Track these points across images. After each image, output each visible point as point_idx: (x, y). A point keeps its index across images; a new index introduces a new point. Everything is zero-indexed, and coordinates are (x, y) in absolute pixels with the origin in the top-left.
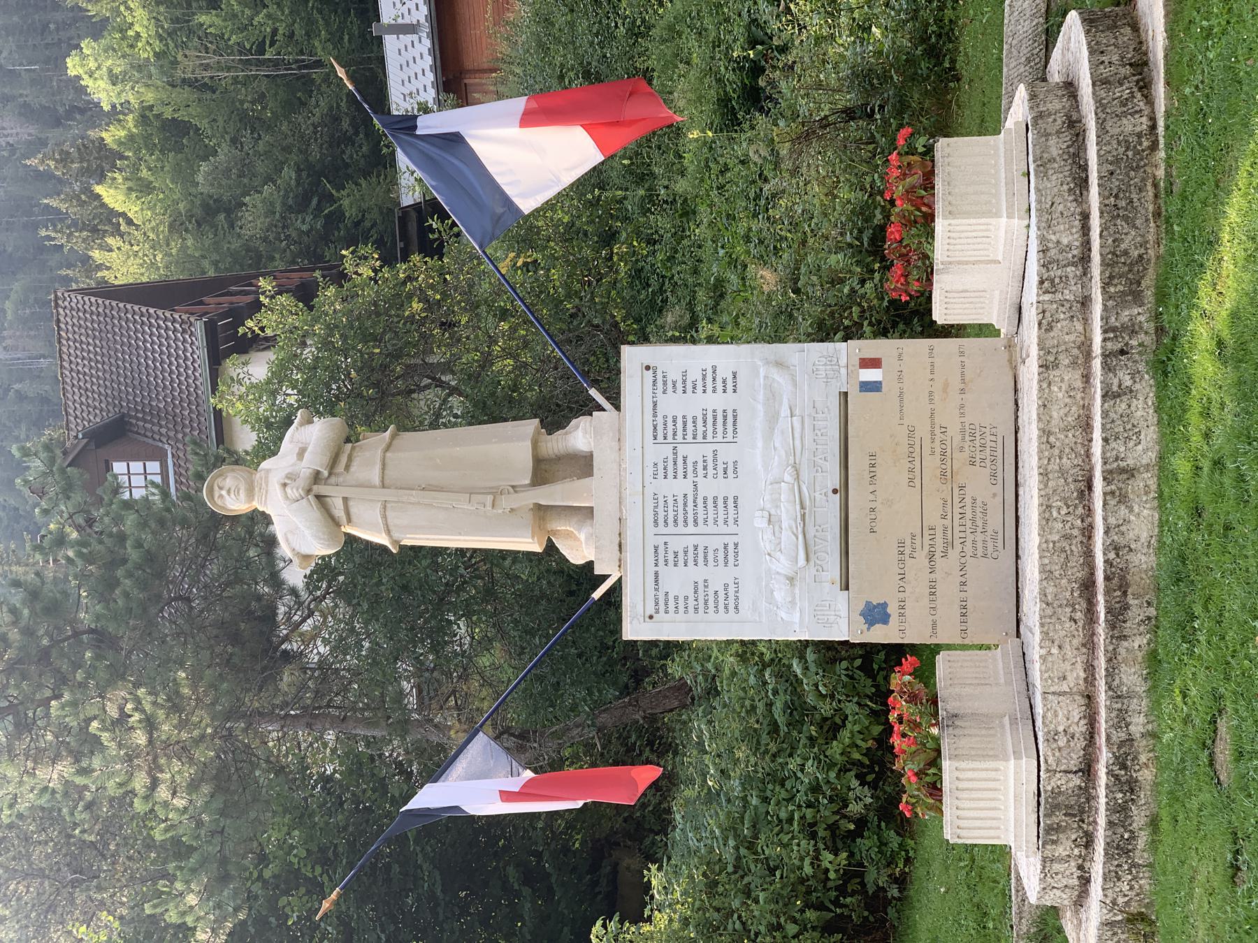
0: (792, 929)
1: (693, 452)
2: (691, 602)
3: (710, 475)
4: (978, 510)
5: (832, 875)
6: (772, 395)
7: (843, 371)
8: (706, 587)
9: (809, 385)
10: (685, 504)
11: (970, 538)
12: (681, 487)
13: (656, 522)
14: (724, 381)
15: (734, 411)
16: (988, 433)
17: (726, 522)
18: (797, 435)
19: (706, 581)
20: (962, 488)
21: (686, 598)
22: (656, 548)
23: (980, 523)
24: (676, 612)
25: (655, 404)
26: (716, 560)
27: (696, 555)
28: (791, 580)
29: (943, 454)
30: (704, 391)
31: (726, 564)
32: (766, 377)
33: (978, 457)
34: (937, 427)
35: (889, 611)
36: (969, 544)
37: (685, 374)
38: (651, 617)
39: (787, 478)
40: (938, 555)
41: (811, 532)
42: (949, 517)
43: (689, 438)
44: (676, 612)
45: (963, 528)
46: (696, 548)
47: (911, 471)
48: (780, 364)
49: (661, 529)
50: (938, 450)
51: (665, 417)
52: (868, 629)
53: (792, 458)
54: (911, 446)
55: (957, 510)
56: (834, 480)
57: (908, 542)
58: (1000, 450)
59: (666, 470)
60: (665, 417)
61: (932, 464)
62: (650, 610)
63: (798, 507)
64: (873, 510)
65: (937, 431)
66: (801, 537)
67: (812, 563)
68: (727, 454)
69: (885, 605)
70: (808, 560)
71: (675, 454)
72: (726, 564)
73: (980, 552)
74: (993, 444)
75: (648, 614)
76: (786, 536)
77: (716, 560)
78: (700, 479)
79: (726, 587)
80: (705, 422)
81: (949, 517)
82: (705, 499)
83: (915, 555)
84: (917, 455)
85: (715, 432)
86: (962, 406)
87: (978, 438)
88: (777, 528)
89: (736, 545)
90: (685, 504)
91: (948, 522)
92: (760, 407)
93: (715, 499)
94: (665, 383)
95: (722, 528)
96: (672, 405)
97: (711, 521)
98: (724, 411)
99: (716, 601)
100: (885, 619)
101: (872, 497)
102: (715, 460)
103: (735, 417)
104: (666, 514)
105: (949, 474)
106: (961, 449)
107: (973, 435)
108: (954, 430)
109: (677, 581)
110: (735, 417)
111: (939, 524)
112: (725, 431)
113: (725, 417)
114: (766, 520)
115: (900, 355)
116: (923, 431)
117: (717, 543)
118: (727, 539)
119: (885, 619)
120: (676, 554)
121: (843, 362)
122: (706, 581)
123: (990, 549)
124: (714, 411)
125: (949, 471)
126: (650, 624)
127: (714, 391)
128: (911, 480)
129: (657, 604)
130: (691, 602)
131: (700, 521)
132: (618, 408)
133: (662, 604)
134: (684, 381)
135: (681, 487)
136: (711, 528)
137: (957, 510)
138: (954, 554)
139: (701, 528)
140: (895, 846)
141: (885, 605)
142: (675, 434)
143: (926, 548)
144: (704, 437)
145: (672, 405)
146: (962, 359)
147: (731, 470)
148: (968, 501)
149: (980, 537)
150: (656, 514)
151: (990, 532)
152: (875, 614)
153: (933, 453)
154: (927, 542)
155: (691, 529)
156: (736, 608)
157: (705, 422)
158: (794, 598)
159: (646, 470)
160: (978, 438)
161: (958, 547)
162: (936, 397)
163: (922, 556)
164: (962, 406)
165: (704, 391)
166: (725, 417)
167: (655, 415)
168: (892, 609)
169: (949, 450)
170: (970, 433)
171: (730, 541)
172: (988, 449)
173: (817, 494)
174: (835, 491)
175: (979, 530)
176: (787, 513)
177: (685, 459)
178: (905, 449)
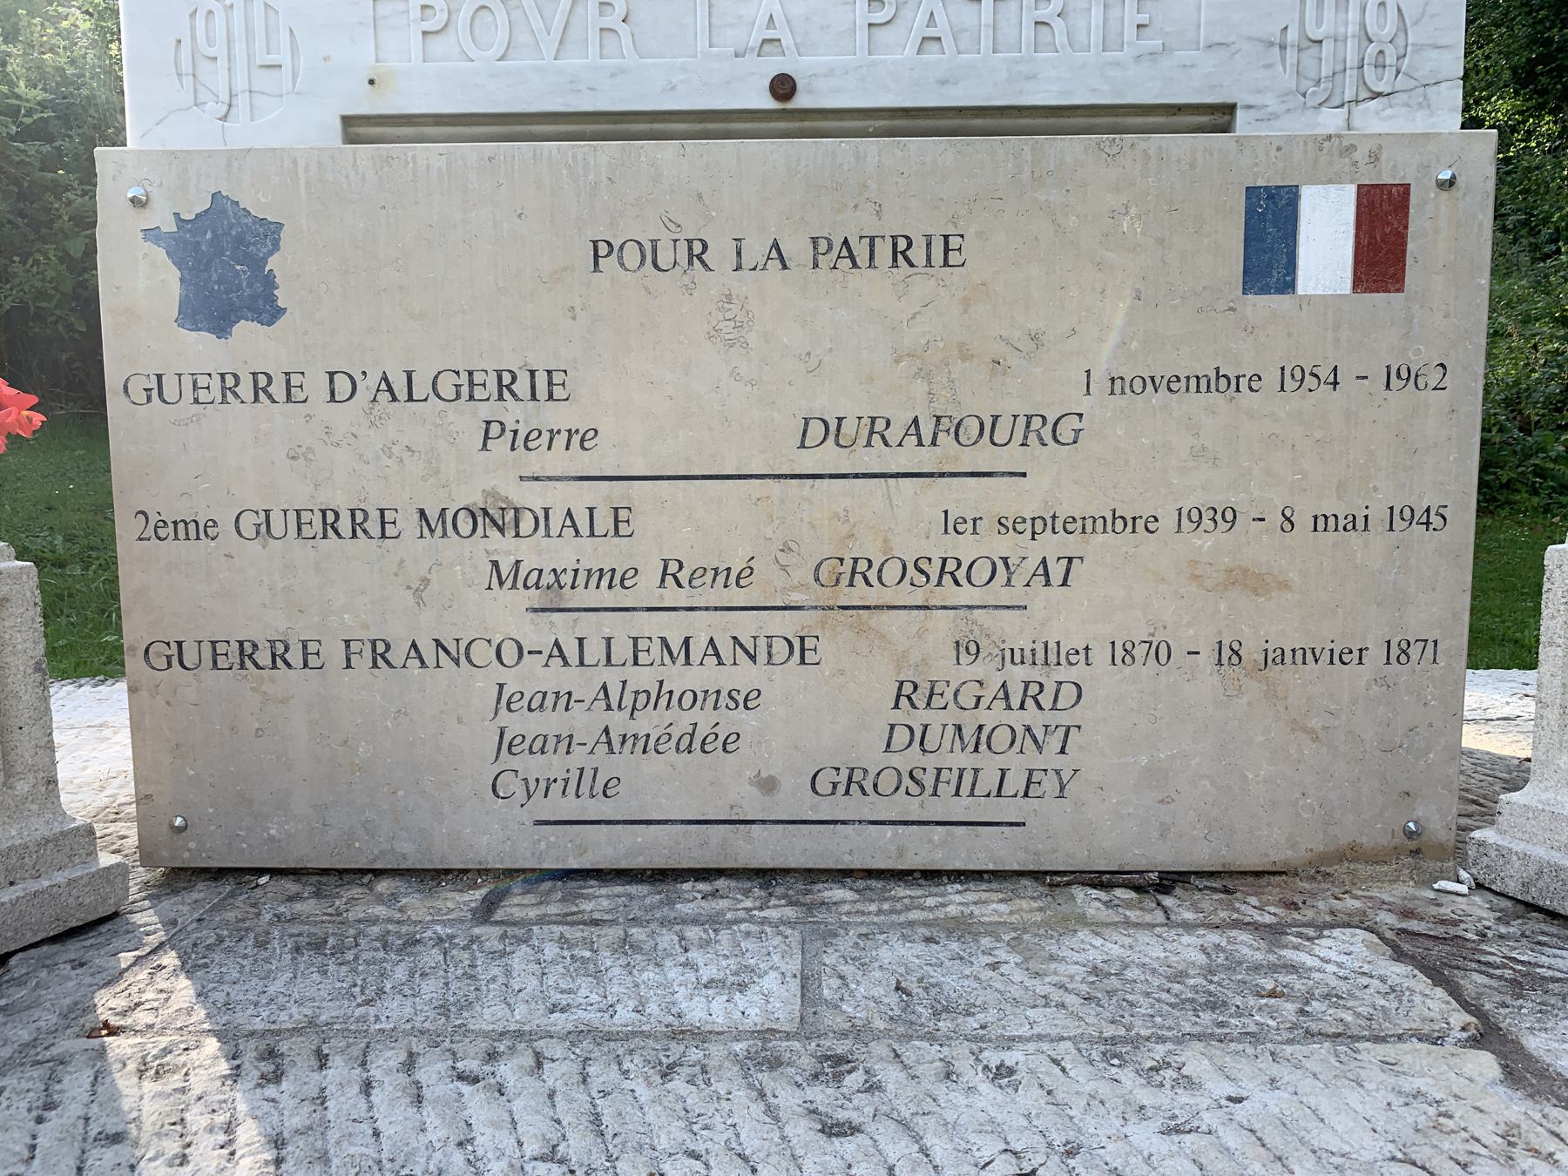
4: (704, 719)
11: (583, 683)
16: (1038, 762)
20: (800, 649)
23: (648, 722)
29: (950, 571)
33: (935, 718)
34: (1072, 544)
35: (244, 329)
36: (555, 678)
40: (504, 548)
42: (672, 596)
45: (622, 651)
47: (876, 429)
50: (966, 548)
52: (152, 234)
54: (988, 429)
55: (701, 628)
57: (557, 416)
58: (961, 808)
61: (904, 520)
64: (697, 254)
65: (1052, 545)
69: (269, 312)
73: (519, 723)
74: (989, 781)
81: (672, 596)
83: (500, 447)
84: (948, 453)
86: (1159, 652)
87: (1017, 719)
91: (647, 588)
101: (756, 250)
105: (860, 594)
106: (968, 648)
107: (1032, 695)
108: (1063, 617)
111: (643, 551)
115: (1411, 377)
116: (1052, 482)
121: (1374, 120)
123: (534, 766)
125: (873, 595)
128: (833, 430)
137: (701, 628)
138: (508, 615)
141: (269, 312)
143: (533, 497)
146: (1376, 654)
148: (743, 676)
149: (585, 722)
151: (611, 766)
152: (229, 269)
153: (952, 525)
154: (559, 497)
160: (1017, 719)
161: (537, 633)
162: (1205, 542)
163: (494, 476)
164: (1159, 652)
168: (251, 345)
169: (966, 595)
170: (1043, 686)
172: (965, 760)
174: (783, 87)
175: (619, 722)
178: (976, 398)
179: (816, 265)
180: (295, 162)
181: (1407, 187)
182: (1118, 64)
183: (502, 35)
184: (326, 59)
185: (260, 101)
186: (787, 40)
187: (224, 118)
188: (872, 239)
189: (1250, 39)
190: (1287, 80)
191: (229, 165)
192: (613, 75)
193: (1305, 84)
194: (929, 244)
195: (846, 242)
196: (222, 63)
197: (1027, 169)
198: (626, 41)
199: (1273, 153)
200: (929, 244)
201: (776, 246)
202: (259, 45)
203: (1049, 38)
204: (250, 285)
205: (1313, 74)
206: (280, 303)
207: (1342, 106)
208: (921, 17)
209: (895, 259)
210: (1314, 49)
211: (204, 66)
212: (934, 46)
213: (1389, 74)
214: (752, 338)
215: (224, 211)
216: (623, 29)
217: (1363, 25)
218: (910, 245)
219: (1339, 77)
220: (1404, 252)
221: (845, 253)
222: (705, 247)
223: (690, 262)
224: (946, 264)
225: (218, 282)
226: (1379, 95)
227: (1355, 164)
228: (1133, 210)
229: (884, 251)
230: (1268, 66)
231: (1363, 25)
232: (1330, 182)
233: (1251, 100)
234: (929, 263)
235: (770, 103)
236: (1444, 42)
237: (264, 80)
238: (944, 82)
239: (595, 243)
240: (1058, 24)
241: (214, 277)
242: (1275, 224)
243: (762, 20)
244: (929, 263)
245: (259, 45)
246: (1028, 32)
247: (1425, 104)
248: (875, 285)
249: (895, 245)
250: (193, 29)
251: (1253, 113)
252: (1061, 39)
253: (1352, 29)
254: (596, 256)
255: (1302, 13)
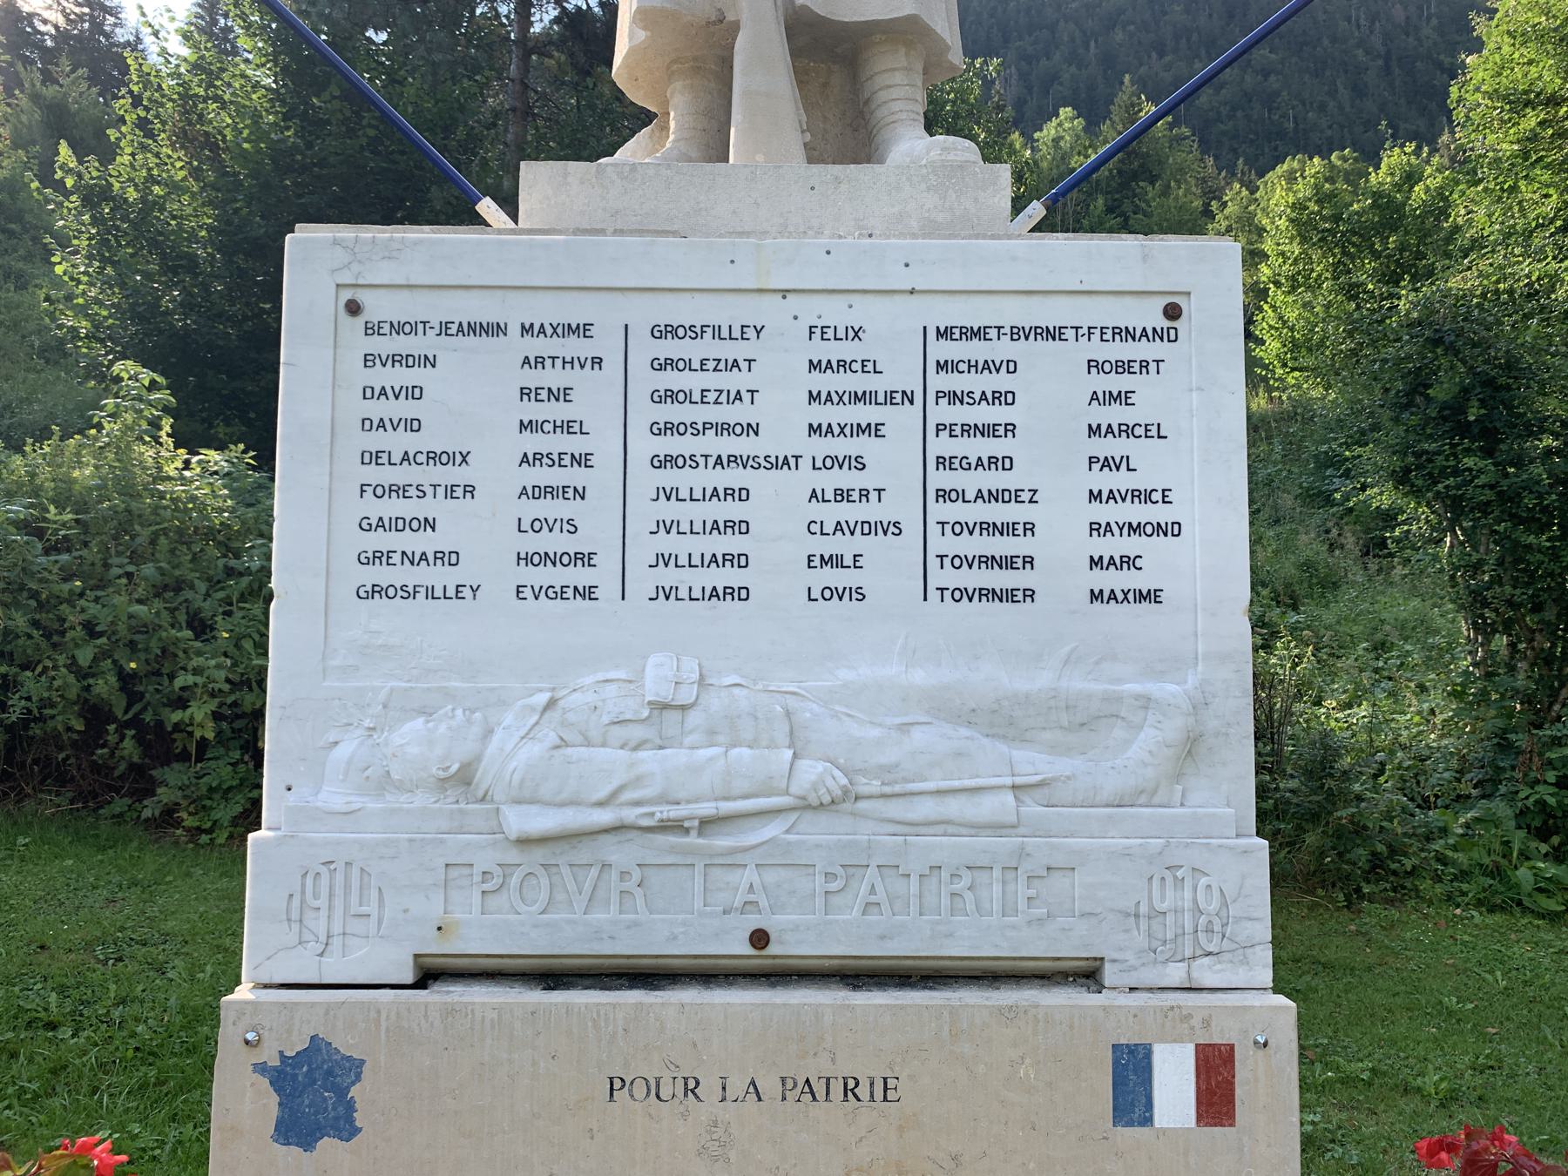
0: (85, 656)
1: (894, 459)
2: (398, 442)
3: (818, 511)
5: (176, 716)
6: (1085, 721)
7: (1175, 974)
8: (450, 492)
9: (1127, 854)
10: (724, 429)
12: (783, 418)
13: (670, 331)
14: (1129, 562)
15: (1029, 594)
17: (664, 560)
18: (954, 807)
19: (469, 490)
21: (414, 425)
22: (583, 330)
24: (368, 393)
25: (1054, 334)
26: (538, 526)
27: (557, 461)
28: (463, 778)
30: (1095, 496)
31: (526, 559)
32: (1146, 702)
37: (1154, 432)
38: (353, 308)
39: (811, 773)
41: (621, 853)
43: (942, 445)
44: (368, 393)
46: (582, 460)
48: (1191, 749)
49: (645, 349)
51: (1012, 367)
52: (261, 1068)
53: (875, 786)
56: (797, 940)
59: (838, 365)
60: (1012, 367)
62: (378, 307)
63: (707, 809)
64: (691, 1088)
66: (604, 817)
67: (513, 856)
68: (888, 567)
70: (525, 842)
71: (890, 398)
72: (526, 559)
75: (364, 297)
76: (607, 765)
77: (538, 526)
78: (806, 479)
79: (448, 558)
80: (995, 496)
82: (742, 495)
85: (960, 528)
88: (637, 732)
89: (588, 593)
90: (724, 429)
92: (1041, 680)
93: (740, 527)
94: (1123, 367)
95: (643, 548)
96: (1051, 388)
97: (669, 510)
98: (1029, 561)
99: (398, 524)
100: (297, 1129)
101: (737, 1086)
102: (869, 528)
103: (1008, 596)
104: (693, 362)
109: (471, 399)
110: (1008, 596)
112: (962, 562)
113: (1008, 563)
114: (666, 693)
117: (596, 525)
118: (608, 562)
119: (297, 1129)
120: (561, 395)
121: (1207, 974)
122: (469, 490)
124: (1029, 528)
126: (328, 304)
127: (1094, 528)
129: (398, 328)
130: (398, 442)
131: (669, 477)
132: (1037, 228)
133: (397, 350)
134: (1127, 430)
135: (783, 418)
136: (644, 512)
139: (645, 480)
140: (216, 815)
142: (954, 397)
144: (942, 495)
145: (1051, 388)
147: (835, 580)
150: (695, 332)
152: (315, 1093)
155: (645, 446)
156: (376, 591)
157: (995, 496)
158: (400, 787)
159: (840, 302)
165: (1095, 496)
166: (1008, 563)
167: (1017, 333)
171: (603, 575)
173: (750, 875)
174: (760, 938)
176: (689, 770)
177: (874, 430)
179: (784, 1099)
180: (379, 1012)
181: (1232, 1047)
182: (1014, 927)
183: (544, 896)
184: (406, 911)
185: (351, 941)
186: (763, 903)
187: (321, 955)
188: (828, 1079)
189: (1112, 910)
190: (1141, 940)
191: (327, 1013)
192: (629, 927)
193: (1155, 944)
194: (872, 1084)
195: (808, 1081)
196: (324, 913)
197: (946, 1028)
198: (640, 902)
199: (1131, 1019)
200: (872, 1084)
201: (753, 1083)
202: (354, 899)
203: (961, 905)
204: (334, 1109)
205: (1160, 936)
206: (358, 1124)
207: (1182, 960)
208: (864, 888)
209: (846, 1095)
210: (1160, 919)
211: (309, 915)
212: (876, 910)
213: (1217, 938)
214: (733, 1155)
215: (319, 1050)
216: (638, 892)
217: (1195, 901)
218: (857, 1085)
219: (1180, 939)
220: (1233, 1095)
221: (807, 1089)
222: (698, 1083)
223: (686, 1095)
224: (885, 1099)
225: (309, 1106)
226: (1210, 954)
227: (1192, 1028)
228: (1028, 1061)
229: (837, 1089)
230: (1127, 931)
231: (1195, 901)
232: (1175, 1041)
233: (1115, 955)
234: (872, 1098)
235: (748, 950)
236: (1255, 915)
237: (356, 926)
238: (882, 937)
239: (611, 1079)
240: (969, 896)
241: (307, 1102)
242: (1135, 1072)
243: (744, 886)
244: (872, 1098)
245: (354, 899)
246: (945, 901)
247: (1245, 961)
248: (831, 1112)
249: (846, 1084)
250: (303, 885)
251: (1117, 966)
252: (970, 907)
253: (1188, 904)
254: (612, 1089)
255: (1150, 892)
